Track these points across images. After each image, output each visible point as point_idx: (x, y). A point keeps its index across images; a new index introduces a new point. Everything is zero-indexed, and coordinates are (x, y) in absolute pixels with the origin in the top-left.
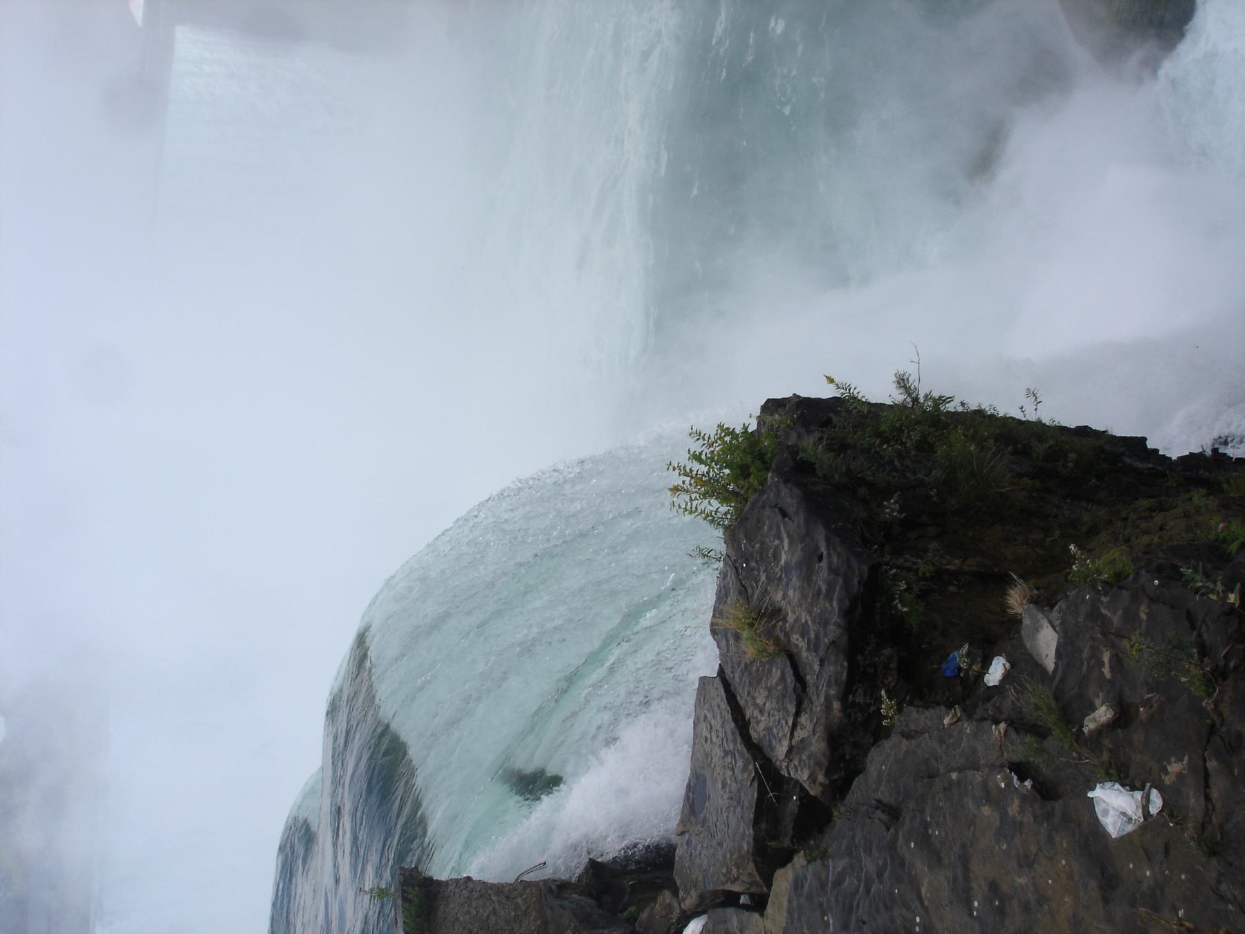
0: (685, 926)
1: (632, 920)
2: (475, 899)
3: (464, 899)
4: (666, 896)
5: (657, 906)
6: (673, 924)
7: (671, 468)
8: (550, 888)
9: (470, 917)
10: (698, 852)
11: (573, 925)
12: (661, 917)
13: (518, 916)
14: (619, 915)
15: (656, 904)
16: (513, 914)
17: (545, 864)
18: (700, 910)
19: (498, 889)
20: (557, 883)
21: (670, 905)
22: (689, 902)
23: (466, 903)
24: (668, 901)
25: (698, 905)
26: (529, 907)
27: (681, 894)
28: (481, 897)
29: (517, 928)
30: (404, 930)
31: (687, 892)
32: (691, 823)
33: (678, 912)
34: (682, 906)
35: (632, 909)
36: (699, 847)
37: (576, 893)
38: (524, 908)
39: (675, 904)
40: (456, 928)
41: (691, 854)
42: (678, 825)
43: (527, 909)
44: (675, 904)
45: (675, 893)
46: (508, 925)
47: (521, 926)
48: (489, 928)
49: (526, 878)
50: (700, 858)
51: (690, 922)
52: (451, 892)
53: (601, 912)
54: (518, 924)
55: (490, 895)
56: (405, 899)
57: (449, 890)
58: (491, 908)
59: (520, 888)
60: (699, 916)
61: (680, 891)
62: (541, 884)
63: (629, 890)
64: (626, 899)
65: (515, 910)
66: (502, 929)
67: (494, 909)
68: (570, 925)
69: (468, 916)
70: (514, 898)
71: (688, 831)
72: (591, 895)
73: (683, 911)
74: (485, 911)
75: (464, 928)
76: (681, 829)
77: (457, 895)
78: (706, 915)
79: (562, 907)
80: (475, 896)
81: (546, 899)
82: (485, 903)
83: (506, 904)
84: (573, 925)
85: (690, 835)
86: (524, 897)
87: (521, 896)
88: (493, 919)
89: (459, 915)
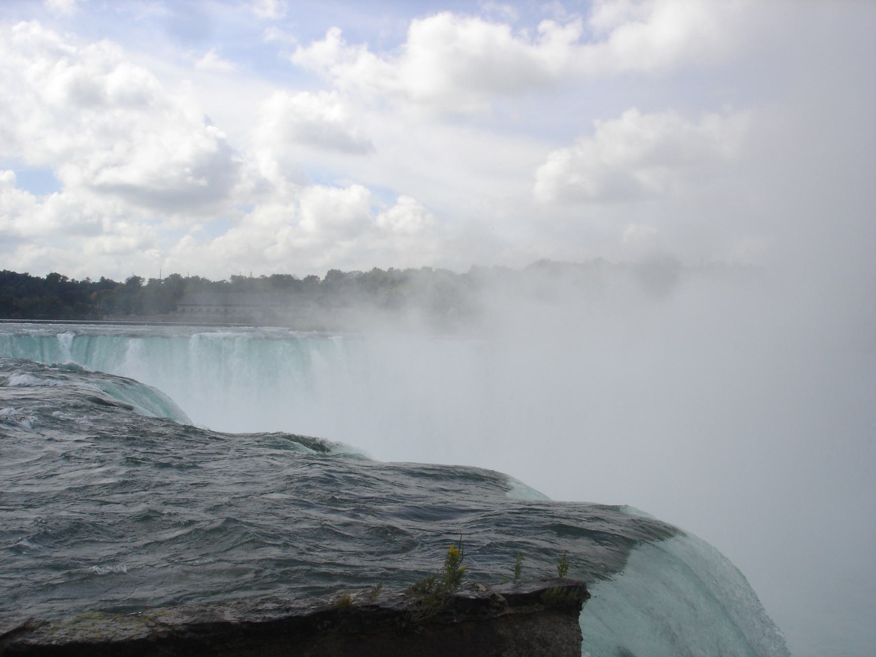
30: (545, 589)
56: (570, 588)
57: (574, 625)
69: (560, 642)
75: (551, 639)
89: (560, 634)
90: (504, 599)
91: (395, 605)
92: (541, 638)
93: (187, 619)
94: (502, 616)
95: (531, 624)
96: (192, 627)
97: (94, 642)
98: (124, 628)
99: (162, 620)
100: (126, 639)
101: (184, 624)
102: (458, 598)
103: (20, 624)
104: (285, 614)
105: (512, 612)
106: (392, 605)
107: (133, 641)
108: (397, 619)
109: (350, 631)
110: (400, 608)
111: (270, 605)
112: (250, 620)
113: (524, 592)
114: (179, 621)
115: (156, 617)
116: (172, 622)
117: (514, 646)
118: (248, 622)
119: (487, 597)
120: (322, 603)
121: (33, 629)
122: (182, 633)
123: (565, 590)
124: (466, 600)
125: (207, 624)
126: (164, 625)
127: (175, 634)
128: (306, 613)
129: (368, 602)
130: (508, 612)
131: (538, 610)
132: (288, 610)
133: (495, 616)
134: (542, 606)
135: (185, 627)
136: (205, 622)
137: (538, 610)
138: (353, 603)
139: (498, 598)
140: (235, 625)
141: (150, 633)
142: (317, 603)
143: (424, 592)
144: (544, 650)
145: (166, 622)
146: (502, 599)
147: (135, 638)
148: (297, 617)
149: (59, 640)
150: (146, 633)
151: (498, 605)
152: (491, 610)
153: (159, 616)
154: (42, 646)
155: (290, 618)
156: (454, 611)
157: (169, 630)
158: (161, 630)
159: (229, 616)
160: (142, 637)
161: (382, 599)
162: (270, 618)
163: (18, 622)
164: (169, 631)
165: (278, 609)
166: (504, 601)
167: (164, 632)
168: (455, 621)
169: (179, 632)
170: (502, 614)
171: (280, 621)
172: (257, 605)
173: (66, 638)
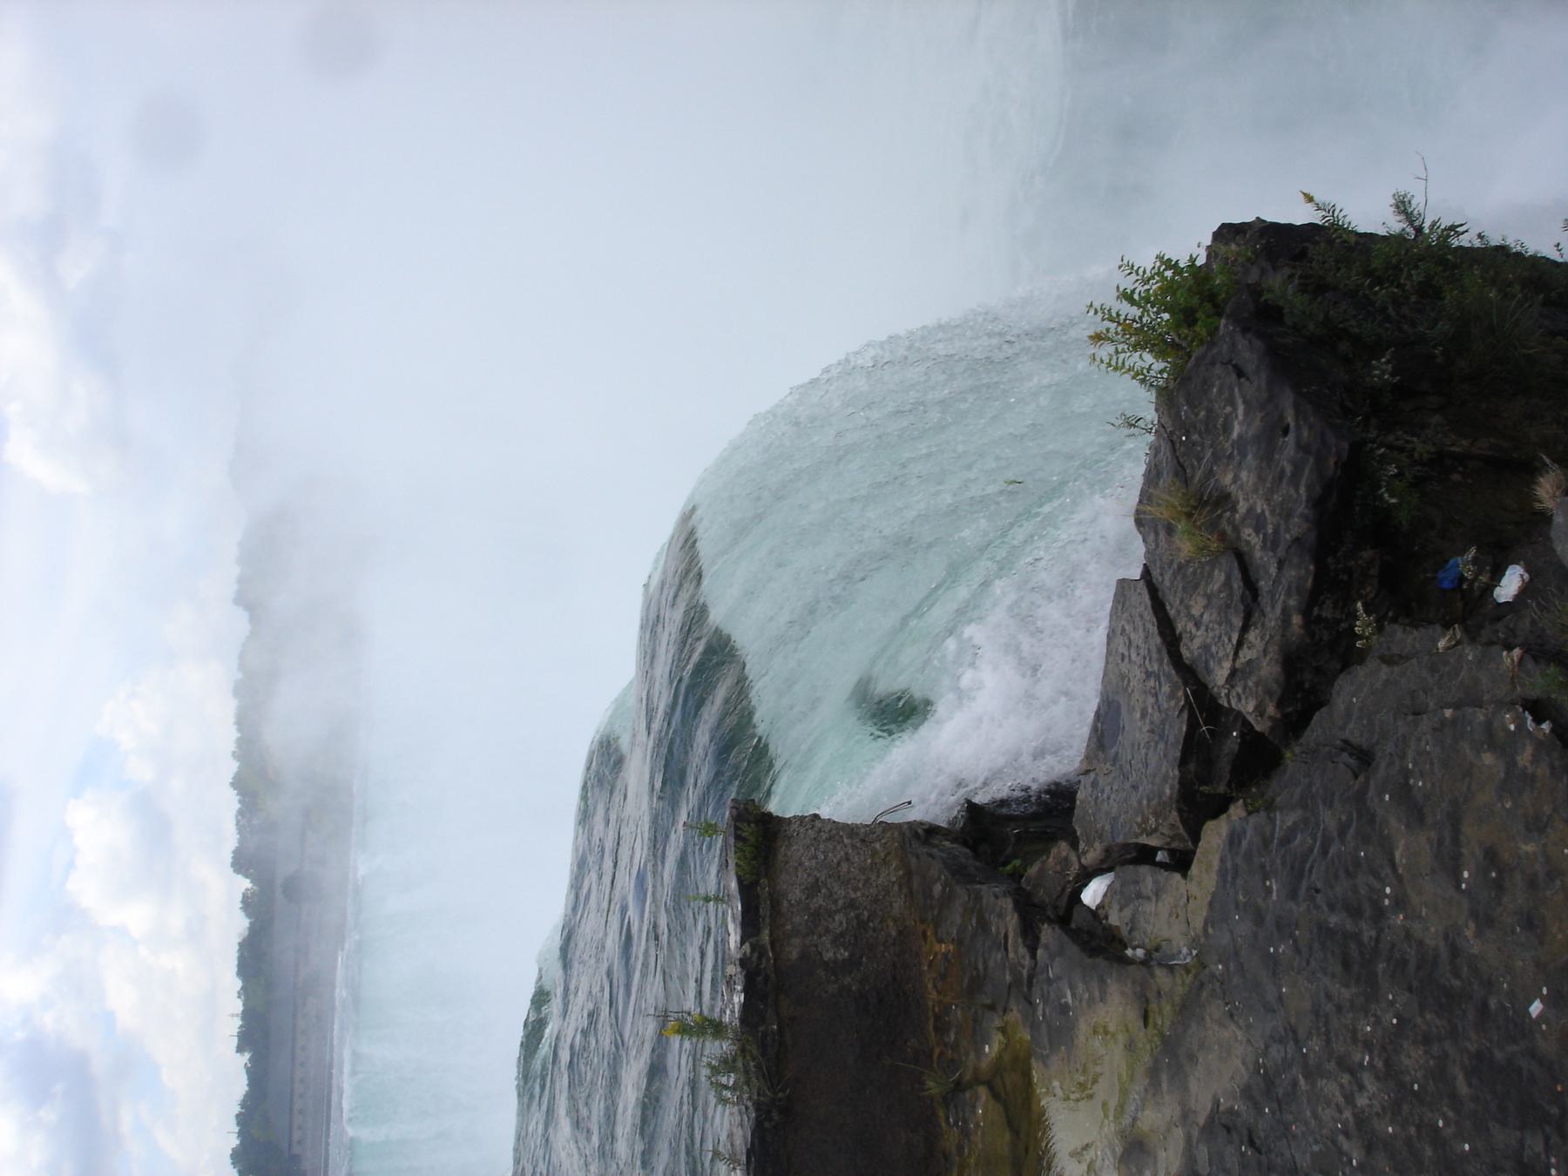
0: (1086, 885)
1: (1016, 876)
2: (824, 841)
3: (811, 840)
4: (1063, 847)
5: (1051, 859)
6: (1069, 882)
7: (1092, 312)
8: (916, 832)
9: (817, 863)
10: (1105, 796)
11: (943, 877)
12: (1056, 872)
13: (876, 864)
14: (1001, 869)
15: (1048, 857)
16: (869, 861)
17: (910, 803)
18: (1104, 866)
19: (852, 830)
20: (925, 827)
21: (1066, 859)
22: (1092, 856)
23: (812, 845)
24: (1064, 854)
25: (1102, 861)
26: (889, 853)
27: (1082, 845)
28: (830, 839)
29: (873, 877)
30: (737, 874)
31: (1090, 843)
32: (1098, 760)
33: (1077, 868)
34: (1083, 861)
35: (1017, 862)
36: (1107, 789)
37: (948, 840)
38: (882, 855)
39: (1074, 858)
40: (800, 875)
41: (1097, 798)
42: (1082, 762)
43: (886, 856)
44: (1074, 858)
45: (1074, 845)
46: (864, 874)
47: (878, 877)
48: (839, 877)
49: (888, 819)
50: (1108, 803)
51: (1090, 881)
52: (794, 831)
53: (978, 864)
54: (876, 874)
55: (842, 837)
56: (738, 838)
57: (792, 829)
58: (842, 853)
59: (879, 830)
60: (1102, 875)
61: (1081, 842)
62: (906, 826)
63: (1013, 840)
64: (1009, 850)
65: (872, 856)
66: (855, 879)
67: (846, 854)
68: (939, 878)
69: (814, 861)
70: (871, 842)
71: (1095, 769)
72: (965, 843)
73: (1082, 867)
74: (835, 856)
75: (809, 875)
76: (1085, 767)
77: (802, 835)
78: (1113, 873)
79: (930, 855)
80: (824, 837)
81: (910, 844)
82: (835, 847)
83: (861, 849)
84: (943, 877)
85: (1097, 774)
86: (883, 841)
87: (880, 840)
88: (845, 866)
89: (803, 858)
90: (747, 944)
92: (806, 892)
94: (772, 948)
95: (785, 904)
105: (767, 932)
108: (767, 1125)
113: (740, 908)
117: (815, 937)
119: (743, 974)
123: (740, 844)
124: (745, 1007)
134: (762, 880)
139: (745, 953)
144: (823, 891)
146: (747, 947)
151: (756, 955)
152: (763, 966)
156: (762, 1028)
161: (740, 1142)
166: (751, 945)
168: (775, 1027)
170: (769, 948)
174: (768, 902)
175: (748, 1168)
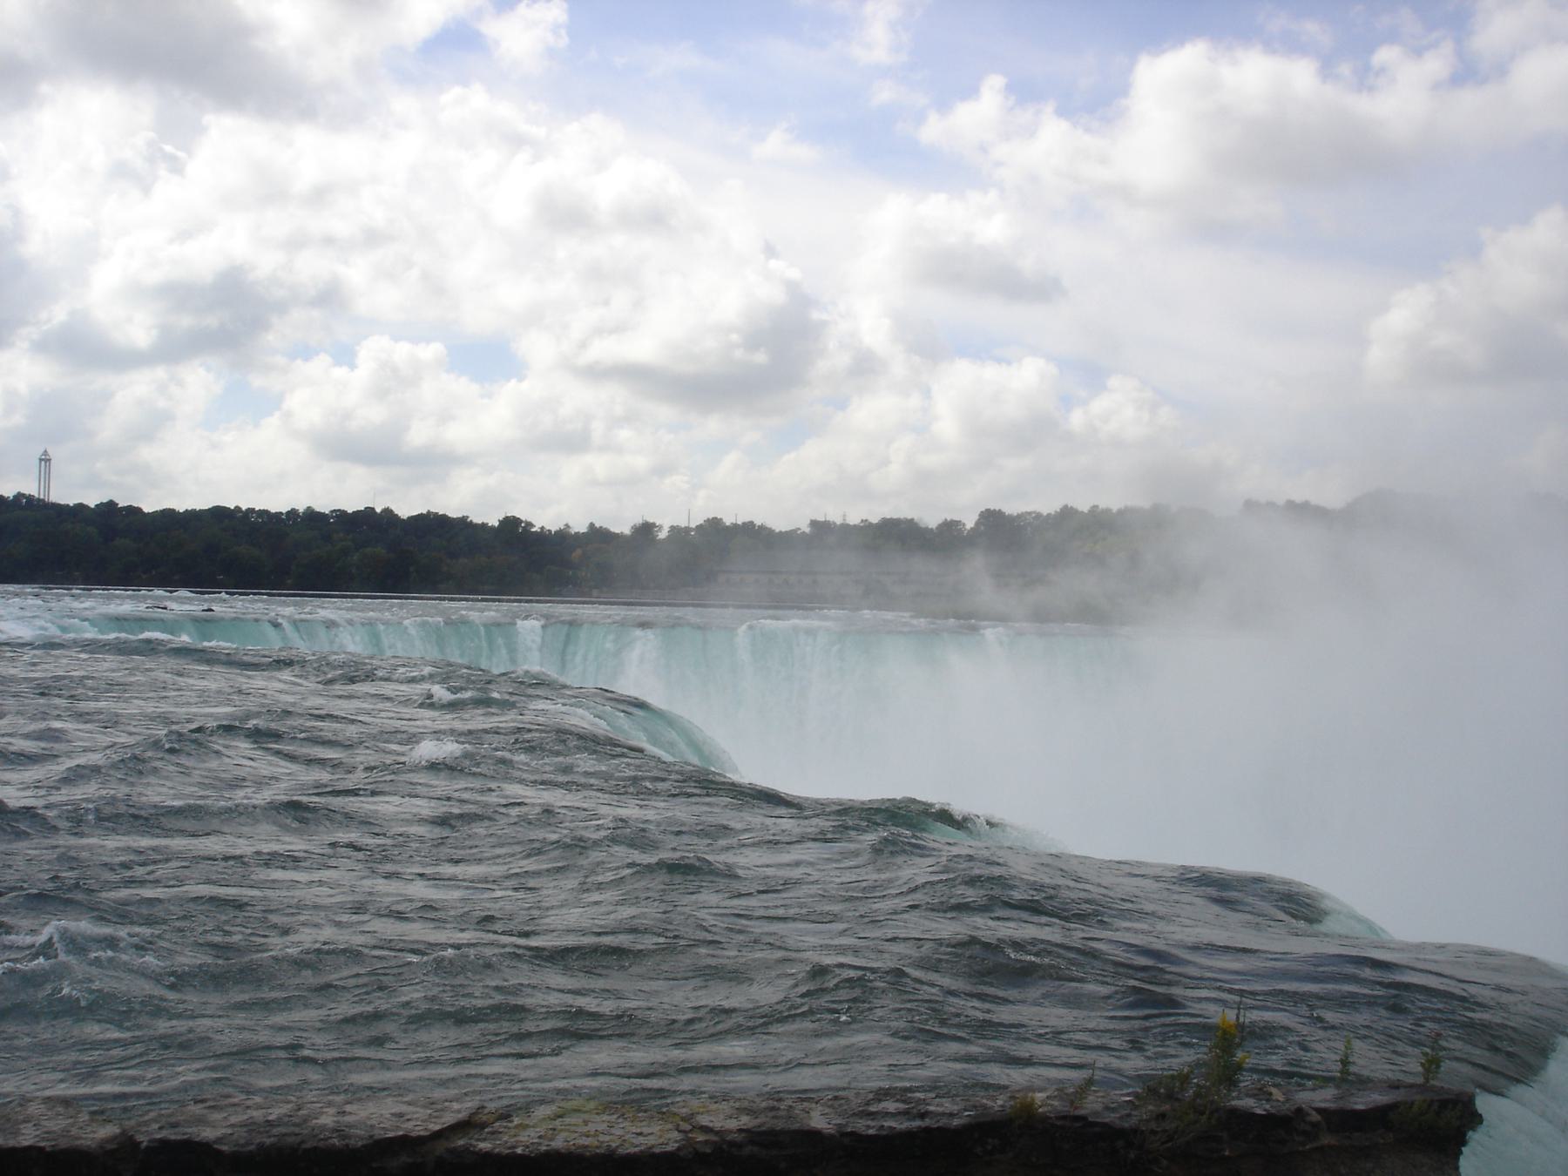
30: (1398, 1102)
56: (1444, 1104)
91: (1115, 1117)
93: (745, 1121)
96: (753, 1136)
97: (588, 1154)
98: (639, 1131)
99: (704, 1120)
100: (641, 1151)
101: (740, 1131)
102: (1234, 1112)
103: (461, 1116)
104: (917, 1123)
106: (1109, 1118)
107: (654, 1155)
109: (1034, 1159)
110: (1126, 1125)
111: (891, 1106)
112: (856, 1130)
114: (732, 1124)
115: (692, 1114)
116: (720, 1125)
118: (852, 1134)
119: (1289, 1113)
120: (985, 1107)
121: (483, 1126)
122: (740, 1146)
124: (1247, 1117)
125: (782, 1132)
126: (706, 1129)
127: (725, 1146)
128: (956, 1122)
129: (1067, 1109)
130: (1326, 1142)
131: (1382, 1141)
132: (922, 1116)
133: (1301, 1149)
134: (1391, 1135)
135: (743, 1135)
136: (778, 1128)
137: (1382, 1141)
138: (1040, 1110)
139: (1308, 1114)
140: (831, 1136)
141: (684, 1142)
142: (975, 1107)
143: (1170, 1096)
145: (711, 1125)
146: (1315, 1117)
147: (657, 1150)
148: (939, 1128)
149: (528, 1147)
150: (676, 1141)
153: (698, 1113)
154: (499, 1155)
155: (927, 1130)
157: (714, 1138)
158: (701, 1138)
159: (819, 1120)
160: (669, 1148)
162: (890, 1127)
163: (459, 1111)
164: (715, 1142)
165: (906, 1113)
167: (706, 1142)
168: (1227, 1153)
169: (732, 1144)
170: (1315, 1145)
171: (909, 1135)
172: (868, 1104)
173: (540, 1144)
174: (1367, 1144)
175: (1064, 1118)
